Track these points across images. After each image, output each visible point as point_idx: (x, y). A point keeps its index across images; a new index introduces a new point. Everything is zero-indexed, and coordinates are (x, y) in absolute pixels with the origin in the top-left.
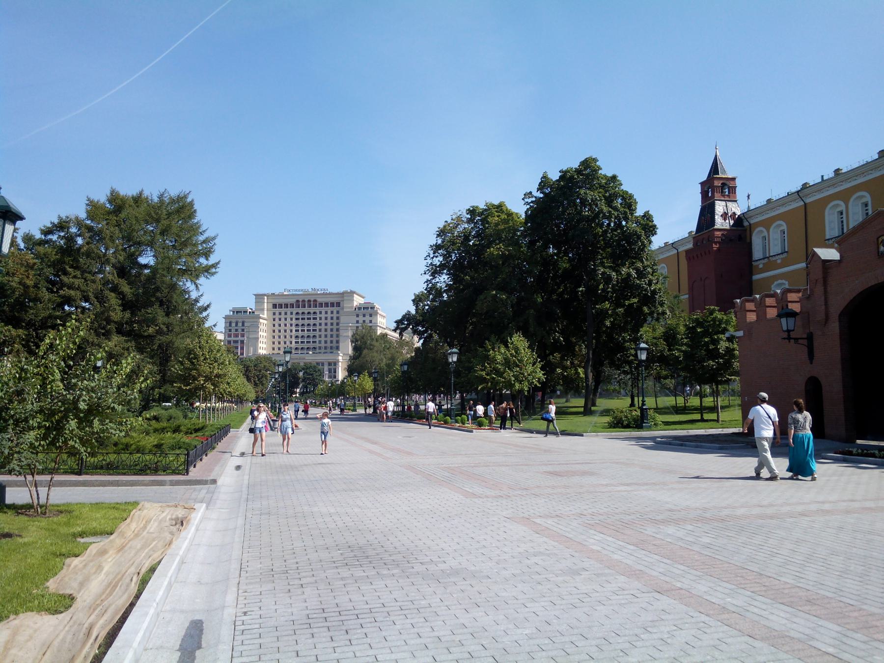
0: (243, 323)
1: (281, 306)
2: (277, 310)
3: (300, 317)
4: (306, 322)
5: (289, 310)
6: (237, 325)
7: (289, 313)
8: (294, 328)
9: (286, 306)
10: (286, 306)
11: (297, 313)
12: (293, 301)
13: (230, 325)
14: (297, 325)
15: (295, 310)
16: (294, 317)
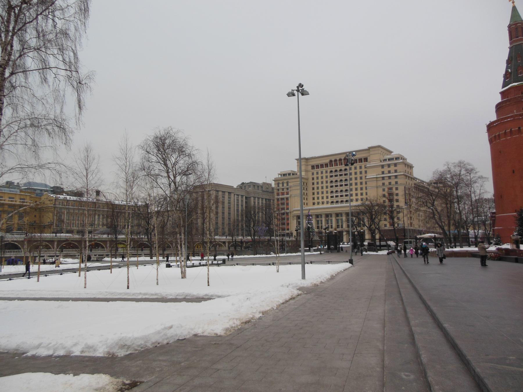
0: (287, 183)
1: (317, 167)
2: (315, 171)
3: (334, 174)
4: (338, 178)
5: (324, 169)
6: (283, 186)
7: (324, 172)
8: (329, 185)
9: (322, 166)
10: (322, 166)
11: (331, 172)
12: (327, 161)
13: (278, 186)
14: (332, 192)
15: (329, 169)
16: (329, 174)
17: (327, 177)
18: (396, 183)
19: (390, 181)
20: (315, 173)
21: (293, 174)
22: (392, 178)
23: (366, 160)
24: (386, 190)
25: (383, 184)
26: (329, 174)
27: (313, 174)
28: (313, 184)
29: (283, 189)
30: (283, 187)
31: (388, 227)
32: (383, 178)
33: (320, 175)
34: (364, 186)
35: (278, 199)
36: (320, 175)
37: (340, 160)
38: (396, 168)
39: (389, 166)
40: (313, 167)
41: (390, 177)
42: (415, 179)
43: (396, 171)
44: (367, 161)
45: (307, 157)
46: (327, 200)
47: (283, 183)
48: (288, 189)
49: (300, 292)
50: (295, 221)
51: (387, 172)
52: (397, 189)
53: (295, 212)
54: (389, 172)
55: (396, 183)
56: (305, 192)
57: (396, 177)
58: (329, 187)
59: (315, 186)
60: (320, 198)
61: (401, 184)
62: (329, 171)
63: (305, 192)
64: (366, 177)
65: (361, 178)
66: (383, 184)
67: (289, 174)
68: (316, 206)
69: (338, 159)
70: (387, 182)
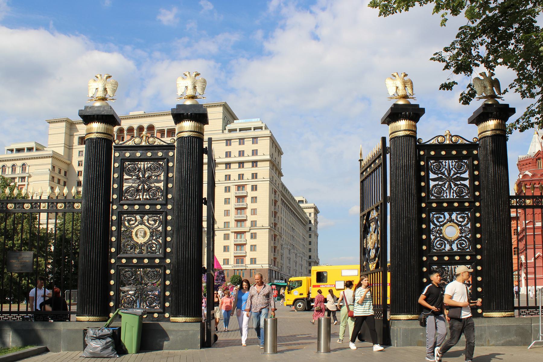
18: (254, 176)
19: (241, 171)
24: (233, 189)
38: (255, 147)
39: (242, 141)
41: (241, 164)
43: (255, 153)
51: (237, 155)
52: (254, 188)
54: (241, 153)
55: (254, 176)
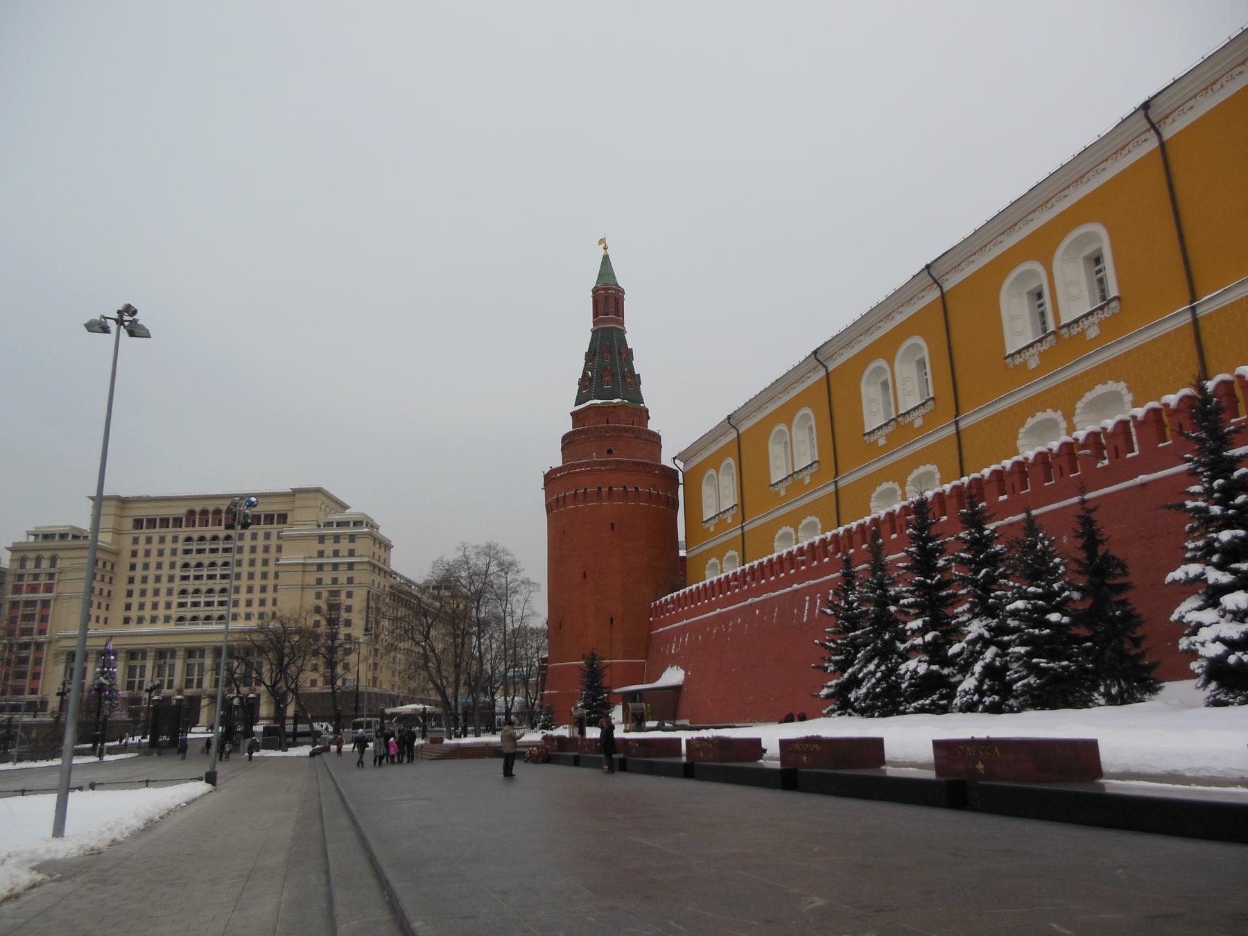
0: (53, 560)
1: (152, 523)
2: (143, 534)
4: (206, 558)
5: (170, 532)
7: (169, 538)
8: (178, 572)
9: (165, 522)
10: (165, 522)
11: (189, 539)
12: (181, 511)
13: (22, 566)
15: (183, 532)
16: (180, 546)
17: (174, 552)
19: (335, 574)
20: (142, 540)
21: (75, 537)
22: (341, 568)
23: (283, 518)
24: (325, 595)
25: (319, 581)
26: (180, 546)
27: (136, 541)
28: (133, 567)
29: (36, 576)
30: (37, 571)
31: (321, 687)
32: (320, 567)
33: (155, 547)
34: (270, 582)
35: (14, 605)
36: (155, 547)
37: (217, 512)
40: (138, 523)
42: (392, 574)
44: (285, 523)
45: (124, 494)
46: (168, 612)
47: (38, 561)
48: (51, 576)
49: (39, 877)
50: (62, 667)
53: (63, 643)
55: (350, 580)
56: (106, 588)
57: (351, 566)
58: (177, 579)
59: (139, 573)
60: (148, 606)
61: (361, 585)
62: (182, 537)
63: (106, 588)
64: (277, 560)
65: (265, 562)
66: (319, 581)
67: (63, 536)
68: (133, 628)
69: (211, 509)
70: (327, 577)
